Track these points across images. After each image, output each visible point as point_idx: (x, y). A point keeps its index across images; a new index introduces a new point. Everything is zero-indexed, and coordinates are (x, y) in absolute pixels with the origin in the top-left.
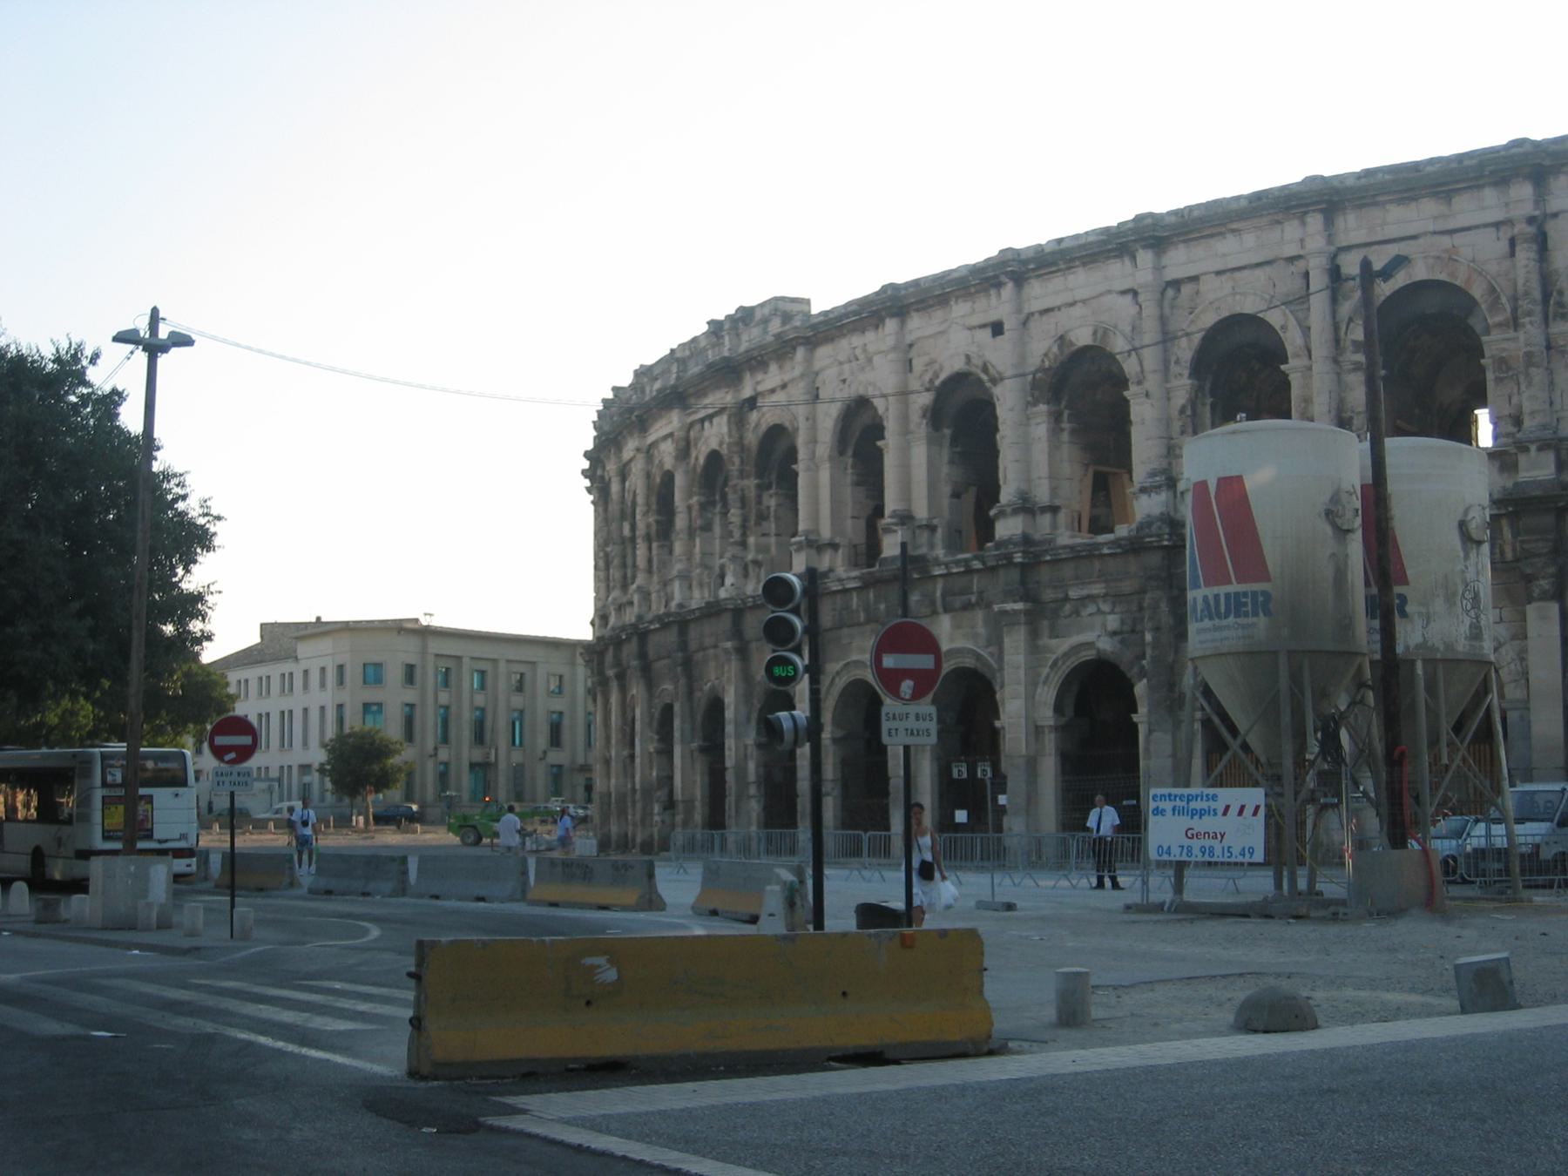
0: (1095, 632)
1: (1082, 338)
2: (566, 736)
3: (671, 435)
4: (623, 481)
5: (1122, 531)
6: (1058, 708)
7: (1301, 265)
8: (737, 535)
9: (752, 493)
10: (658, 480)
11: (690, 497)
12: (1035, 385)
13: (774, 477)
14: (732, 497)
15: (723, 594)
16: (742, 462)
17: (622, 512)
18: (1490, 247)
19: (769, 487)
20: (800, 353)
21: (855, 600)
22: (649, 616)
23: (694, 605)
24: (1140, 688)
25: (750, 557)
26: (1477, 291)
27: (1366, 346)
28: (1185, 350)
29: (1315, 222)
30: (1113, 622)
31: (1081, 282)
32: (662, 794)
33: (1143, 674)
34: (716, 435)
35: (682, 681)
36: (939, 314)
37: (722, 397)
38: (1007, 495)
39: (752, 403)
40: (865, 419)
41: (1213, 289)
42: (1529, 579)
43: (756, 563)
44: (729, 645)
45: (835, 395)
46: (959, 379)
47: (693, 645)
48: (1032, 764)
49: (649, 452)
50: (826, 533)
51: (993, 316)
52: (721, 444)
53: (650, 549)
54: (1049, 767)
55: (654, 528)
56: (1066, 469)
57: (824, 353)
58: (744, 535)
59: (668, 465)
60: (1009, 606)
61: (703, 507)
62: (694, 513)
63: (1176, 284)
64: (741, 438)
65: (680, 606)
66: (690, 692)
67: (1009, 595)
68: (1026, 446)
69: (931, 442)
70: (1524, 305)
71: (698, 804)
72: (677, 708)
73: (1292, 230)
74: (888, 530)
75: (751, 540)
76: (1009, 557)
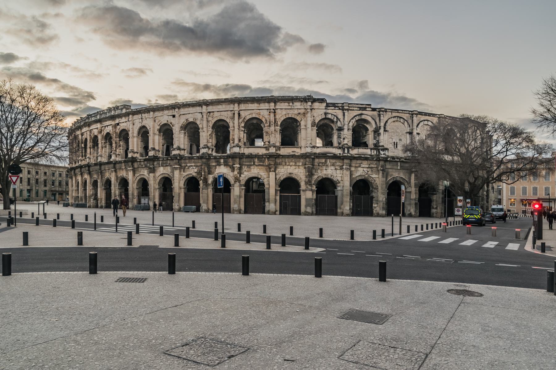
0: (192, 171)
1: (191, 120)
2: (55, 184)
3: (97, 128)
4: (82, 136)
5: (198, 155)
6: (184, 185)
7: (233, 112)
8: (114, 149)
12: (181, 127)
14: (114, 142)
15: (111, 160)
18: (266, 113)
20: (131, 116)
21: (142, 163)
24: (201, 182)
26: (264, 120)
27: (244, 127)
28: (211, 125)
29: (236, 105)
30: (196, 170)
31: (191, 110)
33: (201, 180)
34: (109, 129)
36: (162, 112)
37: (113, 123)
38: (174, 147)
39: (118, 124)
40: (144, 130)
41: (216, 114)
42: (270, 168)
45: (138, 125)
46: (165, 124)
47: (103, 169)
48: (179, 194)
49: (91, 131)
50: (135, 150)
51: (174, 114)
54: (182, 195)
56: (186, 143)
57: (136, 117)
59: (96, 134)
60: (176, 166)
63: (210, 112)
66: (102, 178)
67: (176, 164)
68: (179, 138)
69: (159, 135)
70: (271, 123)
72: (99, 181)
73: (232, 106)
74: (150, 151)
75: (117, 150)
76: (176, 158)
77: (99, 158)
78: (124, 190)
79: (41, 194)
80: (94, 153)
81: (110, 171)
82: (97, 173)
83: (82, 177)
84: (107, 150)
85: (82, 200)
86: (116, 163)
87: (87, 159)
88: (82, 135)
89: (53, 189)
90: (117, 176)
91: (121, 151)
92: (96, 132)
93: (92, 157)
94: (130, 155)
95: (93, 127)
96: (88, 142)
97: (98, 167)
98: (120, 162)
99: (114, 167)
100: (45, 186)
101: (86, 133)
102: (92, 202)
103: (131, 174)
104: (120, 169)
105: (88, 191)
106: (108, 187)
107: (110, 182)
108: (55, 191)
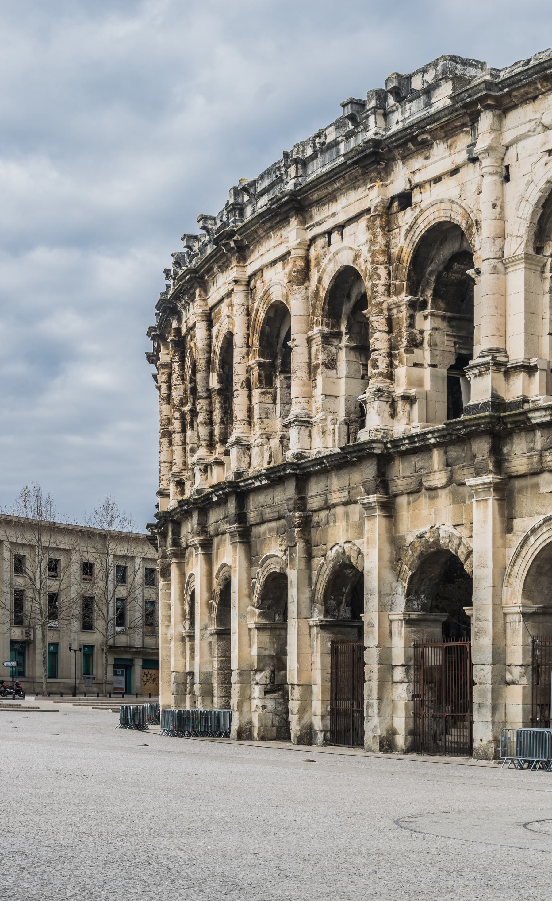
8: (382, 364)
9: (403, 313)
10: (262, 315)
11: (310, 328)
13: (429, 292)
14: (377, 322)
15: (363, 436)
16: (389, 274)
17: (209, 361)
19: (423, 305)
22: (251, 472)
23: (313, 454)
25: (399, 390)
32: (262, 677)
35: (300, 546)
37: (369, 196)
43: (409, 399)
44: (373, 498)
47: (314, 503)
49: (249, 285)
50: (517, 354)
52: (356, 257)
53: (250, 397)
55: (256, 372)
58: (391, 365)
59: (277, 295)
61: (327, 339)
62: (314, 350)
64: (388, 245)
65: (299, 456)
66: (309, 557)
71: (317, 690)
77: (293, 432)
78: (437, 630)
79: (70, 663)
80: (266, 415)
81: (356, 510)
82: (284, 532)
83: (209, 559)
84: (342, 381)
85: (208, 693)
86: (386, 457)
87: (234, 451)
88: (210, 320)
89: (122, 640)
90: (395, 541)
91: (419, 375)
92: (276, 283)
93: (255, 437)
94: (480, 389)
95: (264, 253)
96: (238, 351)
97: (289, 491)
98: (418, 447)
99: (382, 483)
100: (88, 626)
101: (228, 309)
102: (255, 707)
103: (484, 513)
104: (415, 491)
105: (234, 638)
106: (345, 613)
107: (358, 579)
108: (129, 649)
